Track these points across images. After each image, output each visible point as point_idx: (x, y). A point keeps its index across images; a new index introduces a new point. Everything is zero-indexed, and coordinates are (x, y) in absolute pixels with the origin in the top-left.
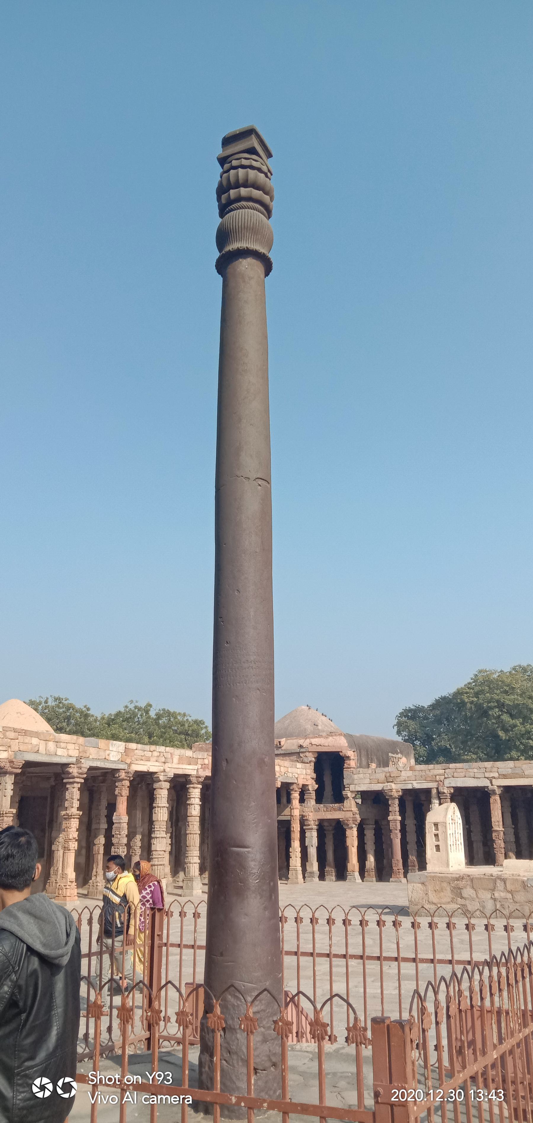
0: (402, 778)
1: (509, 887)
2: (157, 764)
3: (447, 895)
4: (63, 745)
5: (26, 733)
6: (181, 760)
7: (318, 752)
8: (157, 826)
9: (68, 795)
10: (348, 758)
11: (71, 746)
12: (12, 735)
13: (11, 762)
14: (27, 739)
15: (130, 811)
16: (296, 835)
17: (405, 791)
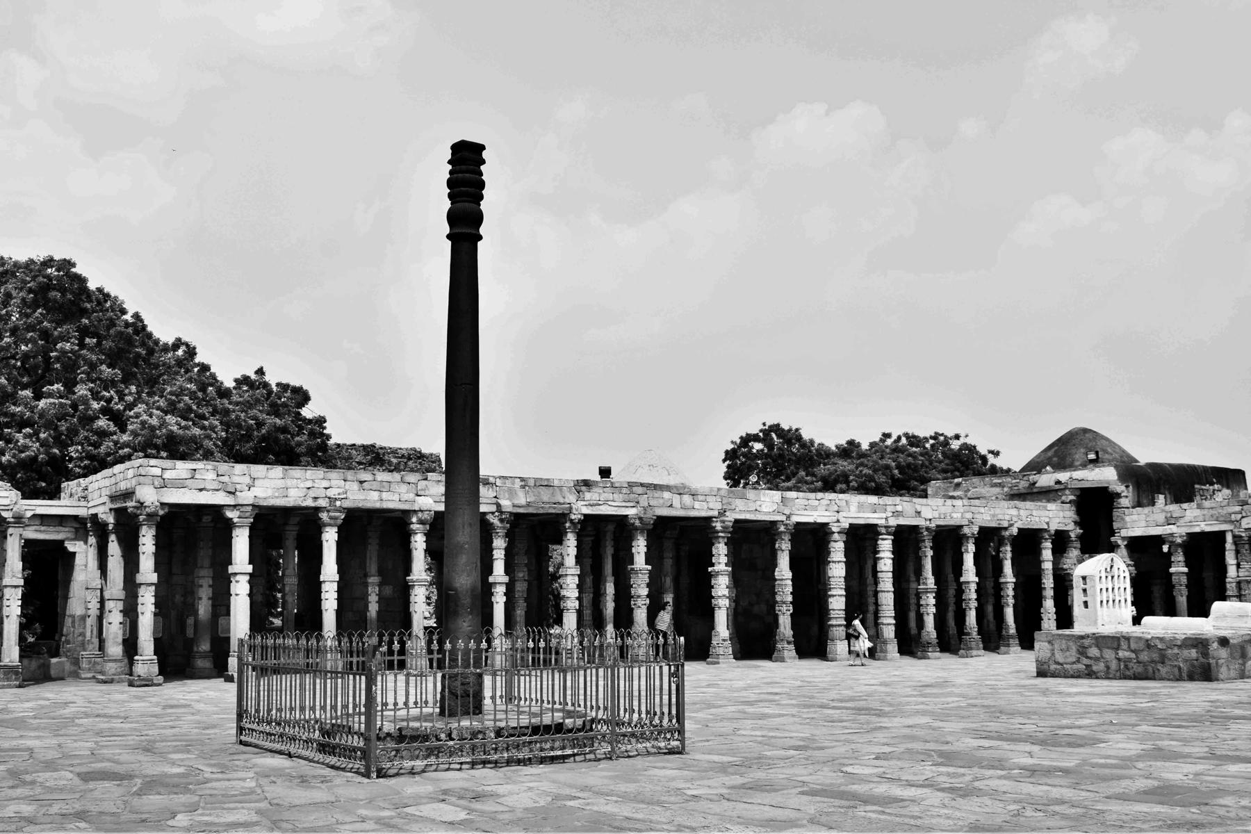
0: (1187, 519)
1: (1133, 646)
2: (827, 513)
3: (1072, 655)
4: (700, 498)
5: (656, 487)
6: (861, 507)
7: (1081, 489)
8: (833, 582)
9: (714, 551)
10: (1118, 495)
11: (709, 498)
12: (640, 490)
13: (640, 519)
14: (657, 494)
15: (793, 567)
16: (1049, 592)
17: (1191, 536)
